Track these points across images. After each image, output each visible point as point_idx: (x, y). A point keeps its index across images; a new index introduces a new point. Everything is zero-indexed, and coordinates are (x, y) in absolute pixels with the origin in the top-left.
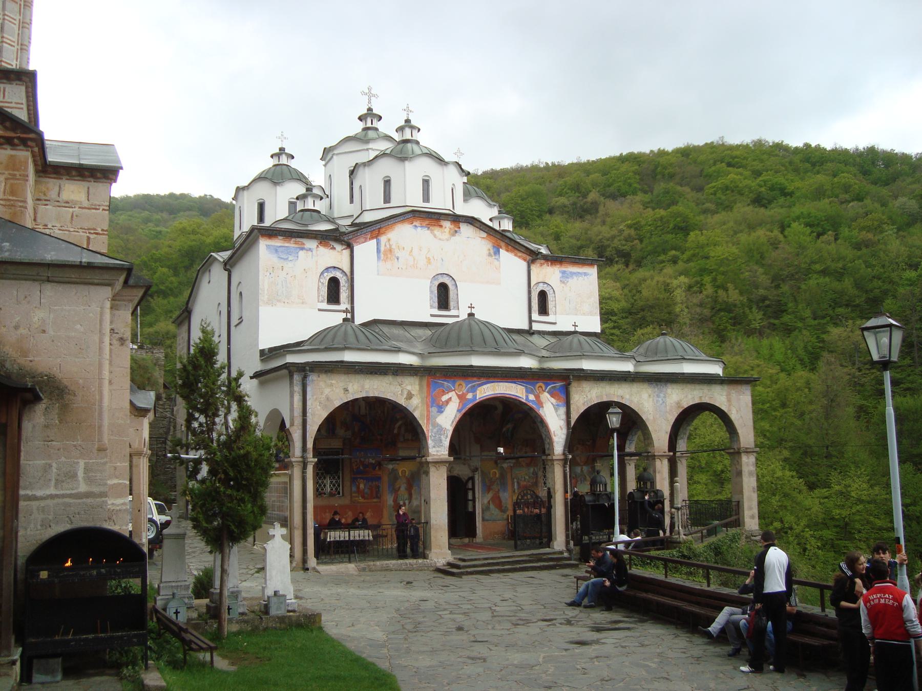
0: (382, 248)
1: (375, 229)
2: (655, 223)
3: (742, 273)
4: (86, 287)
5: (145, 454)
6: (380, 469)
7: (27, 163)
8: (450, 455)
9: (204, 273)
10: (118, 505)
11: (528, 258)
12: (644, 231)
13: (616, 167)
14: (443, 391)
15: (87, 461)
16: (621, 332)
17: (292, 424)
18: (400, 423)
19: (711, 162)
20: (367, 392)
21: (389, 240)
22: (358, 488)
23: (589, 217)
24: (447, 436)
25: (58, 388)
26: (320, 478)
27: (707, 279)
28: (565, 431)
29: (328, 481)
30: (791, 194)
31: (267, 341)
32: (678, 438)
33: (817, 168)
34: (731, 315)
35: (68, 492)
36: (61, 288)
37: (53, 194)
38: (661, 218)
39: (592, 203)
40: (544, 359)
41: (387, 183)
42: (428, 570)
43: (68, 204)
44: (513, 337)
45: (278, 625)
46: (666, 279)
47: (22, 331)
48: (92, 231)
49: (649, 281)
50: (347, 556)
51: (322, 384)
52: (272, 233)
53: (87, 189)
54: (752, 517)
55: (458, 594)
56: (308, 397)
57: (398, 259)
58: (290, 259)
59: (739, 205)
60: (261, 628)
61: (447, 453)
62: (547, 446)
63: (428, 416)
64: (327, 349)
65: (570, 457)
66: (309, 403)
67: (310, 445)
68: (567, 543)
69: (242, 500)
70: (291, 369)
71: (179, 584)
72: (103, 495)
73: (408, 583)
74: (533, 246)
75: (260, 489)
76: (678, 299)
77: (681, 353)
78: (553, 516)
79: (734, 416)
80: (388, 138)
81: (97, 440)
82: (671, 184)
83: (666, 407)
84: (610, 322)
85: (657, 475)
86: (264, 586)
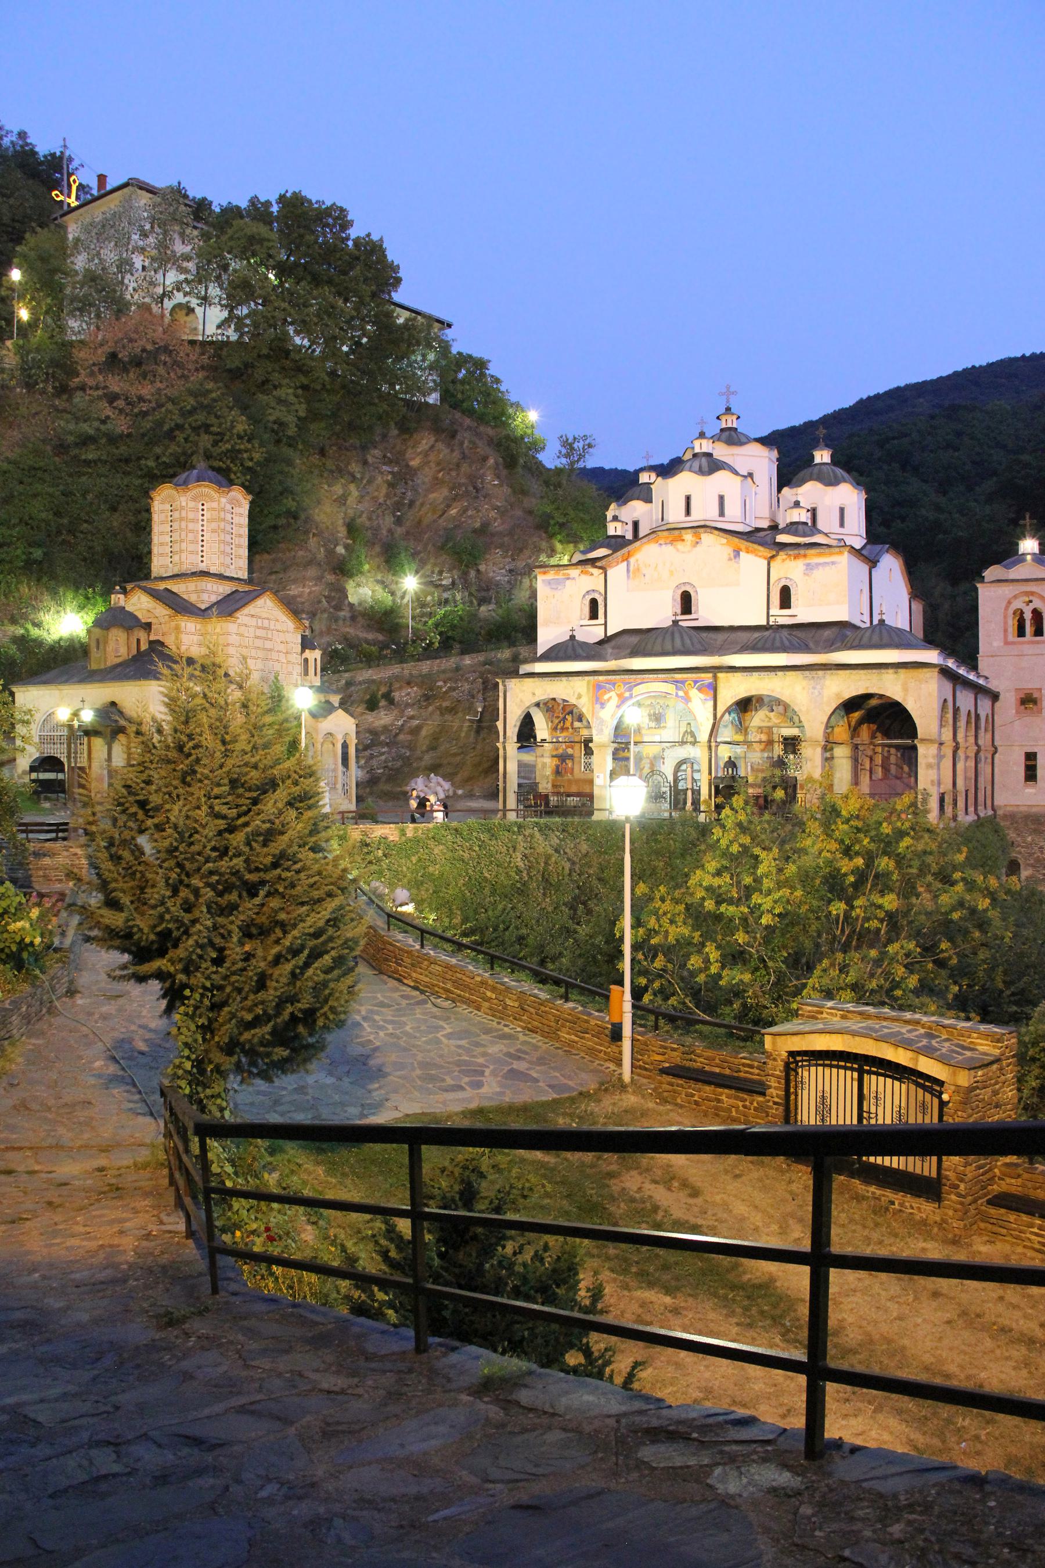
28: (711, 721)
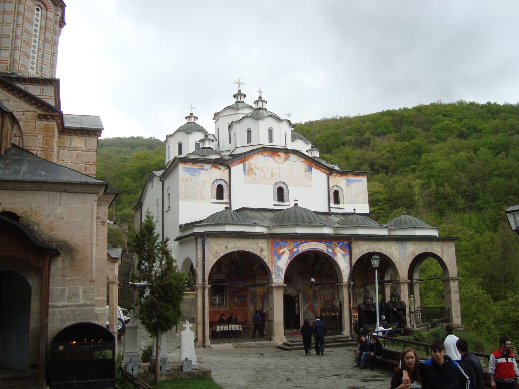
0: (247, 168)
1: (242, 158)
2: (403, 149)
3: (453, 177)
4: (84, 195)
5: (116, 283)
6: (246, 290)
7: (54, 128)
8: (284, 283)
9: (149, 182)
10: (101, 311)
11: (328, 172)
12: (396, 154)
13: (380, 118)
14: (281, 247)
15: (84, 287)
16: (384, 212)
17: (197, 266)
18: (257, 265)
19: (434, 114)
20: (238, 248)
21: (250, 164)
22: (234, 301)
23: (365, 147)
24: (283, 273)
25: (69, 248)
26: (213, 296)
27: (432, 181)
28: (349, 269)
29: (217, 298)
30: (480, 131)
31: (184, 220)
32: (414, 272)
33: (495, 116)
34: (447, 201)
35: (74, 304)
36: (71, 195)
37: (67, 144)
38: (406, 147)
39: (367, 139)
40: (337, 228)
41: (249, 132)
42: (272, 347)
43: (75, 149)
44: (320, 217)
45: (188, 377)
46: (409, 181)
47: (51, 218)
48: (88, 163)
49: (399, 183)
50: (228, 339)
51: (213, 244)
52: (185, 160)
53: (85, 141)
54: (457, 317)
55: (289, 360)
56: (206, 251)
57: (255, 174)
58: (196, 175)
59: (450, 138)
60: (178, 379)
61: (283, 281)
62: (339, 277)
63: (272, 261)
64: (216, 225)
65: (352, 283)
66: (206, 254)
67: (207, 277)
68: (351, 332)
69: (168, 308)
70: (196, 236)
71: (134, 354)
72: (93, 305)
73: (261, 354)
74: (330, 166)
75: (178, 302)
76: (416, 192)
77: (414, 224)
78: (343, 317)
79: (445, 259)
80: (250, 107)
81: (89, 276)
82: (411, 127)
83: (406, 254)
84: (378, 206)
85: (402, 293)
86: (180, 355)
